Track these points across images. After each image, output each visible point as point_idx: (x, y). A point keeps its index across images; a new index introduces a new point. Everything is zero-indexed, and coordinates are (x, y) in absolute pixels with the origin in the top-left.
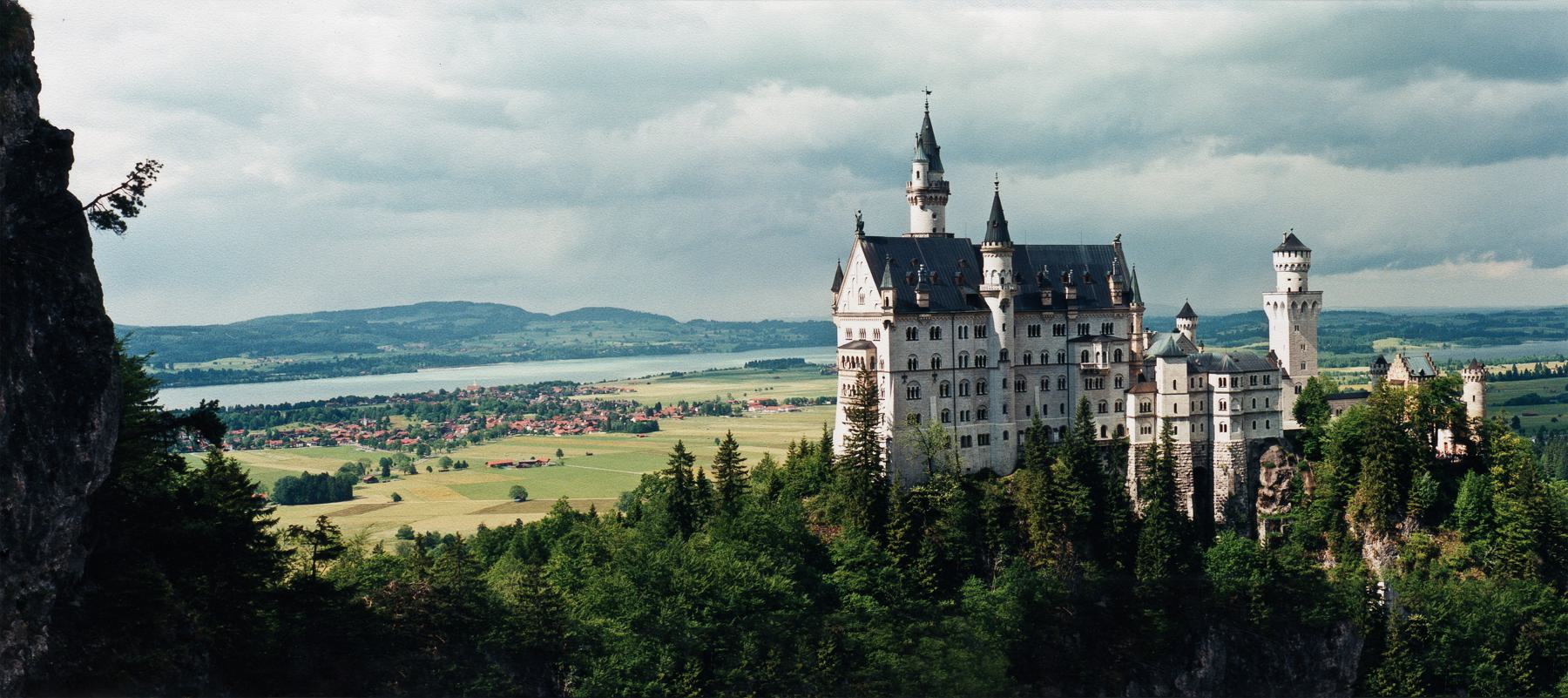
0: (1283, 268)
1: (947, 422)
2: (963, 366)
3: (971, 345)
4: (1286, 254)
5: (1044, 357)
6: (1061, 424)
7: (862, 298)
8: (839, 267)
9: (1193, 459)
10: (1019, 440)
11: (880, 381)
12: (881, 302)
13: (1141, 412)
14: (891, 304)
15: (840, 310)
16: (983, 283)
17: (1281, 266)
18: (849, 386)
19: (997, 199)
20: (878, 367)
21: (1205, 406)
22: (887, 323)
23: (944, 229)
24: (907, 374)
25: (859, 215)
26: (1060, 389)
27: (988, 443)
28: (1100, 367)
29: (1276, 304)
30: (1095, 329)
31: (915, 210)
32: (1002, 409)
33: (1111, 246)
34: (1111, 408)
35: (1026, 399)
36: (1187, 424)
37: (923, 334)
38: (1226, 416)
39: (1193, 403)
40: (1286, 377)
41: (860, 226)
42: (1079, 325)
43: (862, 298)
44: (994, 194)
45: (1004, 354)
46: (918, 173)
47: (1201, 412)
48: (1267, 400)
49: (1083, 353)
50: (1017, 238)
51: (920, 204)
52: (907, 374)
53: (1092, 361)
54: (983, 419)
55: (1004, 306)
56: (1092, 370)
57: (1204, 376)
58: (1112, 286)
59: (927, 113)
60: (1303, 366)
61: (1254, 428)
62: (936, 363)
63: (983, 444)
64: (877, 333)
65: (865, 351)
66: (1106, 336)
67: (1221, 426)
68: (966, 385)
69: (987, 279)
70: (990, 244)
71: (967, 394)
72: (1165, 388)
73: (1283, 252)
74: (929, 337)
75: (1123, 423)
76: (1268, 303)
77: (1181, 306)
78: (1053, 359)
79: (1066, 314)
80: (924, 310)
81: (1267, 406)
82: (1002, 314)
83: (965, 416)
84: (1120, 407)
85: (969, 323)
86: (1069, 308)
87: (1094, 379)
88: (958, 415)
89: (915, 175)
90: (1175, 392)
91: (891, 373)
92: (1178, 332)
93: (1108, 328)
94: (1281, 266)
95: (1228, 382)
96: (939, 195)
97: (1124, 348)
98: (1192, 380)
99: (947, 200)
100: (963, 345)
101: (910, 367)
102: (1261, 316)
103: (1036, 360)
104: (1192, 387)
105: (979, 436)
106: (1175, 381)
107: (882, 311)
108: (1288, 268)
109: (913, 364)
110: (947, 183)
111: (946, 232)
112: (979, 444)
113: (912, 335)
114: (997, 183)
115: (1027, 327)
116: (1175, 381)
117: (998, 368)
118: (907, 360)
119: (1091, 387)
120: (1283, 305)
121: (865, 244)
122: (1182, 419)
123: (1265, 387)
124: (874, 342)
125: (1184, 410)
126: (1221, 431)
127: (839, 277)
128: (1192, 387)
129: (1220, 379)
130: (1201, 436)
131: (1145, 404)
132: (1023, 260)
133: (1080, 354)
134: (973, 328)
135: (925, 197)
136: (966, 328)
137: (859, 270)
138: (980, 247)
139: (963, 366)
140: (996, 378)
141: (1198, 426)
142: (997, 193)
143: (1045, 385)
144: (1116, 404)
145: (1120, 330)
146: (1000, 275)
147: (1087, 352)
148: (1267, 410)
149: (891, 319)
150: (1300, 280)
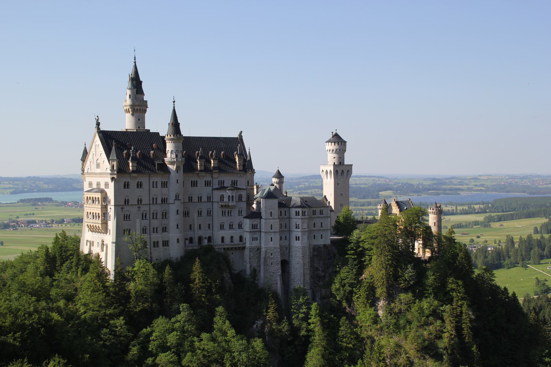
0: (331, 152)
1: (146, 233)
2: (155, 203)
4: (333, 144)
5: (200, 199)
7: (98, 166)
8: (85, 148)
9: (281, 254)
13: (253, 228)
14: (115, 168)
15: (86, 171)
16: (166, 157)
17: (330, 150)
18: (90, 213)
19: (174, 111)
22: (112, 179)
23: (144, 127)
24: (123, 207)
25: (97, 118)
26: (208, 216)
27: (168, 245)
28: (230, 204)
29: (327, 170)
30: (227, 184)
32: (176, 226)
33: (238, 138)
34: (235, 226)
36: (278, 236)
39: (281, 224)
40: (332, 210)
41: (98, 124)
42: (219, 181)
43: (98, 166)
44: (173, 108)
46: (130, 95)
47: (285, 230)
48: (322, 223)
49: (221, 196)
50: (185, 132)
52: (123, 207)
53: (226, 199)
54: (165, 231)
56: (225, 206)
59: (135, 62)
61: (314, 238)
62: (140, 201)
63: (165, 246)
64: (107, 185)
65: (100, 194)
67: (296, 237)
68: (156, 213)
69: (169, 155)
70: (170, 136)
71: (156, 218)
72: (266, 216)
73: (331, 143)
74: (136, 186)
75: (242, 235)
76: (323, 171)
77: (275, 172)
78: (204, 199)
79: (212, 175)
81: (322, 227)
82: (178, 175)
83: (155, 230)
84: (240, 226)
85: (158, 179)
87: (227, 211)
88: (152, 230)
89: (128, 96)
90: (271, 218)
91: (115, 206)
92: (274, 185)
93: (234, 183)
94: (330, 150)
95: (300, 213)
97: (244, 194)
98: (281, 212)
99: (146, 111)
100: (154, 191)
102: (319, 177)
103: (195, 199)
104: (281, 215)
105: (163, 242)
106: (271, 212)
108: (334, 152)
109: (127, 202)
110: (147, 101)
111: (146, 128)
112: (163, 246)
114: (174, 102)
115: (190, 182)
116: (271, 212)
117: (174, 203)
118: (124, 200)
119: (225, 214)
120: (331, 171)
121: (101, 135)
122: (275, 232)
123: (321, 216)
124: (105, 189)
125: (276, 227)
126: (296, 240)
127: (85, 153)
128: (281, 215)
129: (296, 211)
130: (286, 243)
131: (255, 224)
133: (220, 197)
134: (161, 183)
135: (134, 109)
136: (156, 182)
138: (164, 137)
139: (155, 203)
140: (173, 208)
141: (283, 237)
142: (174, 107)
143: (200, 214)
144: (239, 224)
145: (242, 183)
146: (175, 153)
147: (223, 196)
148: (322, 228)
149: (115, 176)
150: (340, 158)
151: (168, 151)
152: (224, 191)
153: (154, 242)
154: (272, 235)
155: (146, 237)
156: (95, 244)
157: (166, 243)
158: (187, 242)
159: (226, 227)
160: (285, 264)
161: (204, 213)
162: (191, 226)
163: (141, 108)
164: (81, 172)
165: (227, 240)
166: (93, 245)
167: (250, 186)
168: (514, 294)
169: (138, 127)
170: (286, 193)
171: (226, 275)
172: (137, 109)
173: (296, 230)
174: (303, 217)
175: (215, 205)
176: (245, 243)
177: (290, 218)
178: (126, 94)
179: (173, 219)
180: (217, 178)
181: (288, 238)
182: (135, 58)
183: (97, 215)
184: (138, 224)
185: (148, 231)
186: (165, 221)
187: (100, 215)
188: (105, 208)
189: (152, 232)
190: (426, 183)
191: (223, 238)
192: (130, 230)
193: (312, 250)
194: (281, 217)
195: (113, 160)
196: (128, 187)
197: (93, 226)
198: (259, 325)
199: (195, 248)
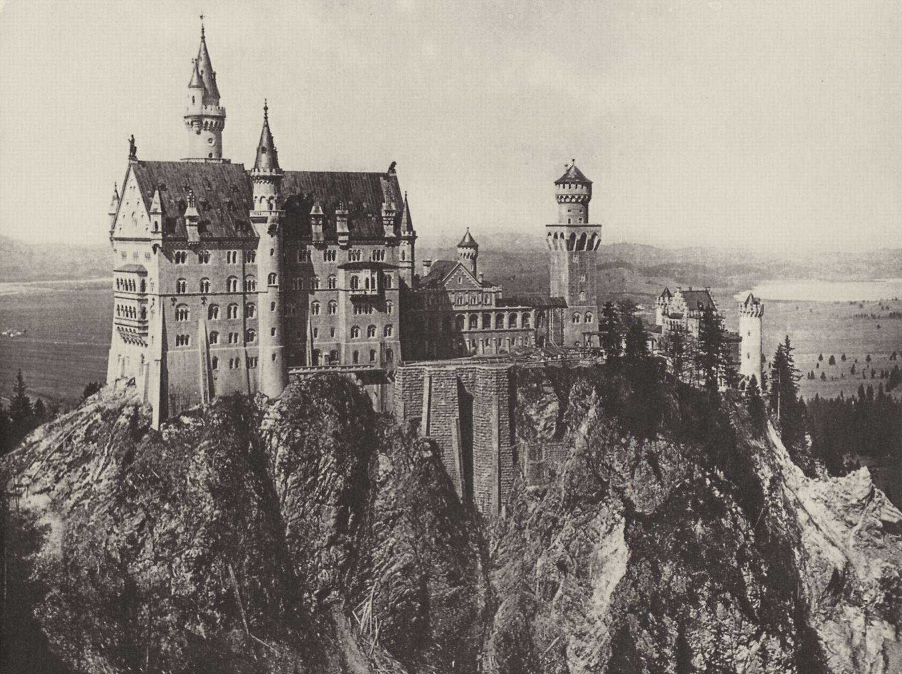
0: (563, 200)
4: (567, 186)
11: (150, 302)
12: (151, 228)
17: (562, 197)
22: (155, 248)
23: (220, 154)
24: (176, 297)
25: (131, 139)
28: (369, 293)
41: (133, 149)
51: (197, 129)
52: (176, 297)
53: (361, 285)
55: (271, 231)
62: (204, 286)
69: (257, 205)
82: (272, 240)
91: (160, 296)
93: (378, 254)
101: (178, 291)
109: (181, 288)
111: (224, 157)
113: (181, 258)
136: (235, 253)
137: (134, 195)
139: (232, 290)
147: (357, 277)
149: (160, 243)
150: (581, 211)
151: (256, 197)
157: (251, 362)
167: (408, 262)
169: (208, 154)
172: (207, 123)
175: (342, 294)
178: (188, 96)
182: (203, 29)
183: (132, 310)
187: (137, 311)
191: (356, 354)
192: (188, 336)
195: (155, 213)
197: (126, 329)
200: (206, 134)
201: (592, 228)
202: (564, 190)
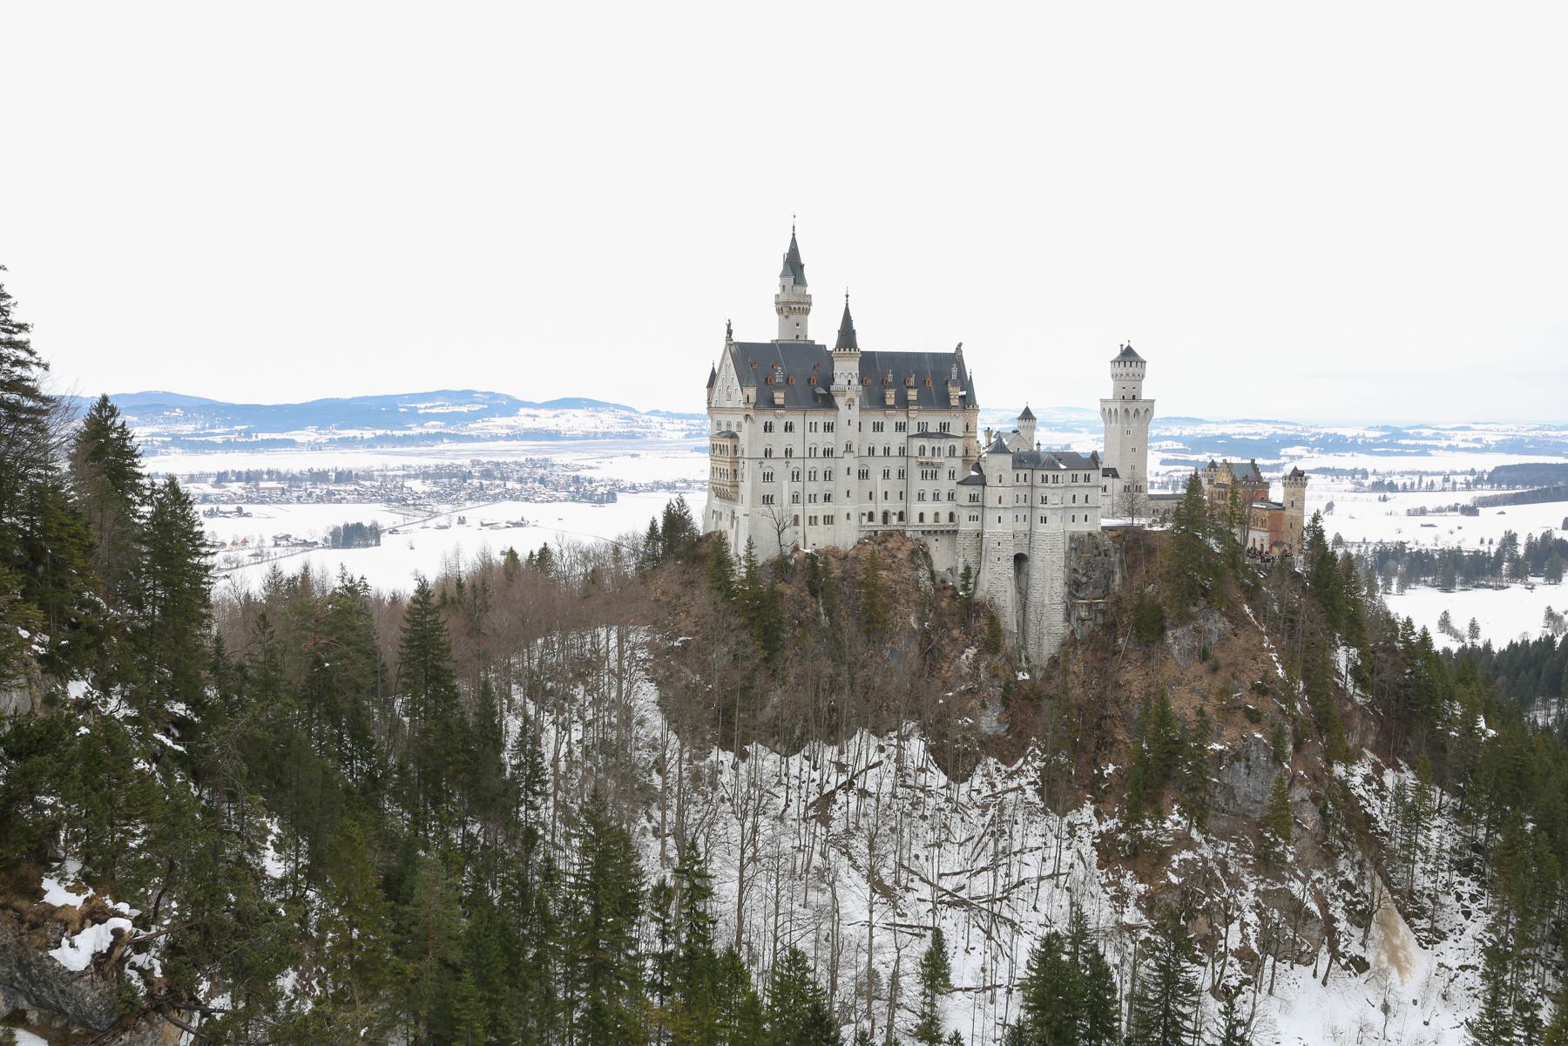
3: (822, 439)
5: (887, 451)
6: (899, 510)
7: (729, 395)
10: (861, 521)
11: (741, 463)
15: (713, 405)
19: (847, 310)
20: (739, 454)
21: (1028, 499)
28: (936, 460)
30: (933, 427)
31: (783, 317)
34: (944, 496)
35: (867, 485)
37: (779, 426)
38: (1048, 509)
41: (730, 332)
43: (729, 395)
45: (849, 448)
48: (1087, 496)
50: (865, 343)
53: (928, 453)
56: (927, 463)
57: (1028, 472)
58: (951, 389)
59: (794, 235)
60: (1133, 467)
62: (788, 453)
64: (739, 425)
66: (943, 432)
69: (837, 380)
75: (954, 510)
78: (894, 451)
80: (780, 407)
81: (1087, 501)
83: (813, 498)
85: (820, 418)
86: (910, 408)
87: (929, 472)
88: (807, 497)
95: (1050, 478)
96: (801, 307)
97: (959, 445)
103: (879, 452)
107: (742, 406)
113: (768, 428)
114: (847, 296)
121: (733, 349)
125: (1008, 500)
130: (1023, 527)
132: (872, 364)
143: (886, 474)
145: (957, 427)
149: (751, 413)
152: (925, 439)
153: (810, 517)
154: (1001, 514)
155: (797, 509)
156: (724, 517)
158: (865, 519)
159: (929, 497)
160: (1020, 560)
161: (894, 474)
162: (871, 493)
163: (801, 307)
164: (706, 405)
165: (929, 519)
166: (721, 519)
168: (1424, 629)
170: (1039, 444)
171: (923, 574)
173: (1041, 506)
174: (1053, 485)
175: (912, 462)
176: (958, 525)
177: (1032, 486)
179: (844, 482)
180: (915, 419)
181: (1028, 518)
184: (785, 488)
185: (801, 500)
186: (828, 486)
188: (735, 461)
189: (807, 501)
190: (1371, 434)
191: (921, 515)
193: (1068, 540)
194: (1018, 484)
196: (770, 431)
198: (971, 656)
199: (876, 529)
200: (794, 318)
201: (1143, 405)
202: (1121, 370)
